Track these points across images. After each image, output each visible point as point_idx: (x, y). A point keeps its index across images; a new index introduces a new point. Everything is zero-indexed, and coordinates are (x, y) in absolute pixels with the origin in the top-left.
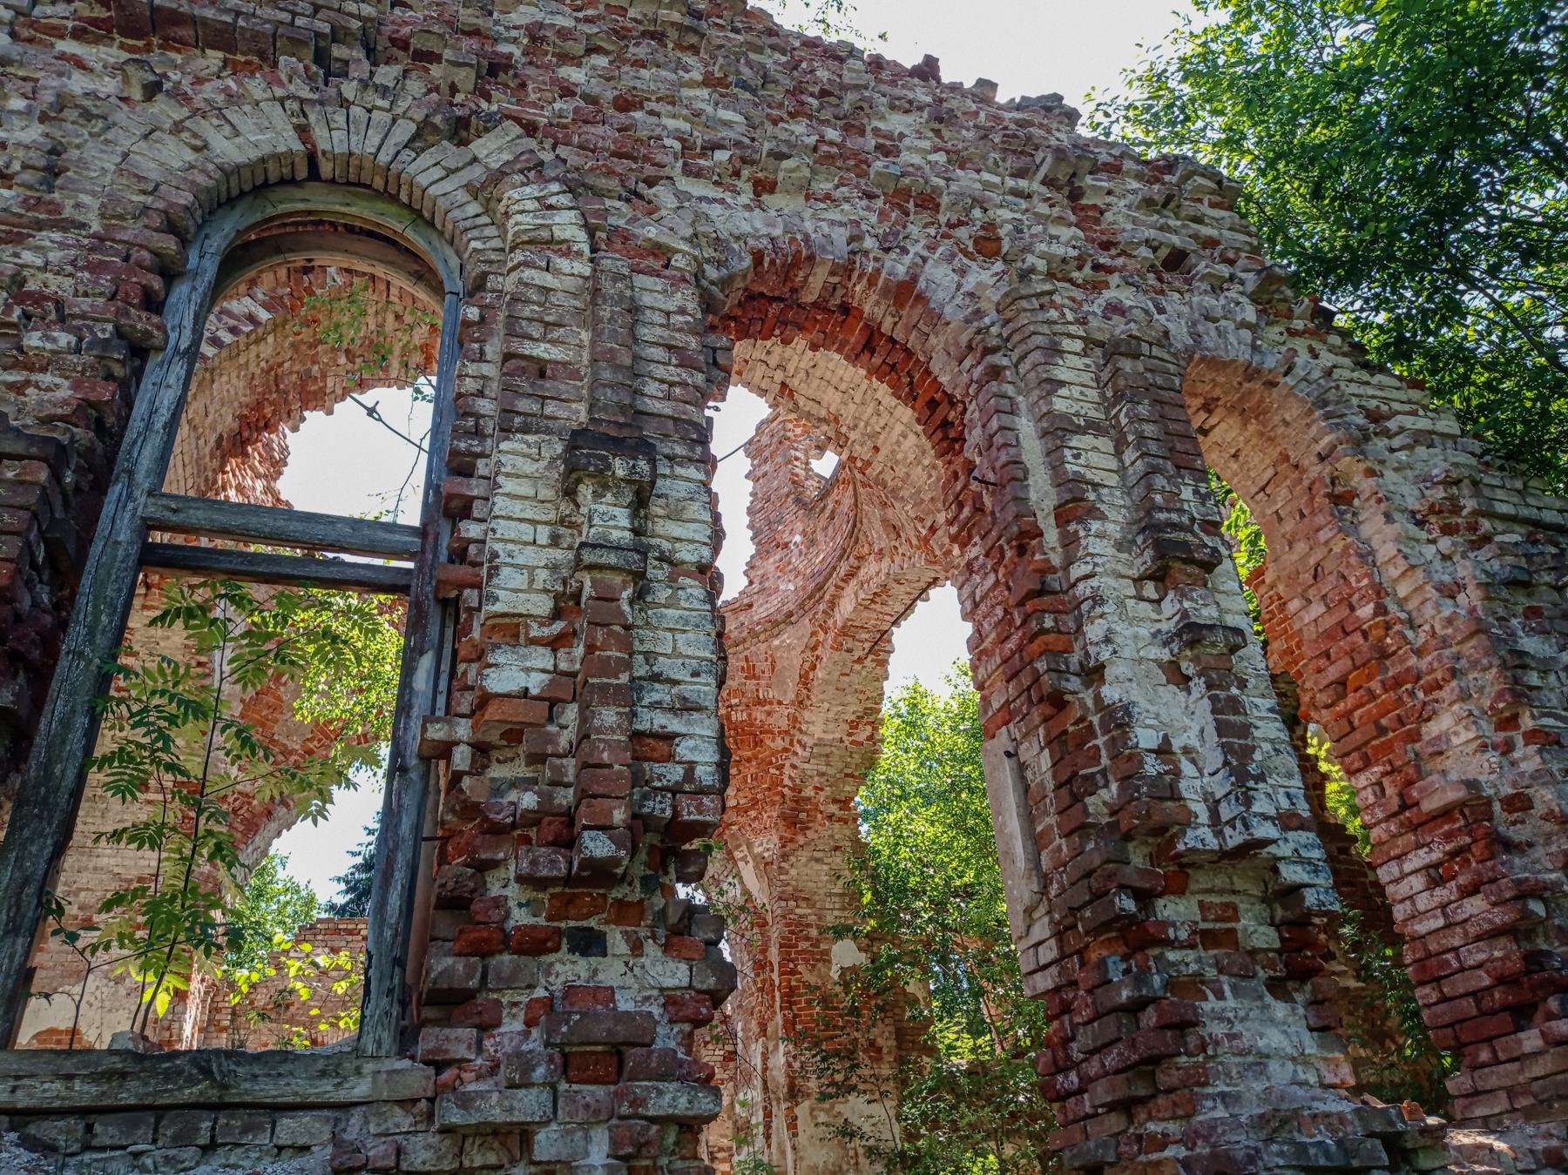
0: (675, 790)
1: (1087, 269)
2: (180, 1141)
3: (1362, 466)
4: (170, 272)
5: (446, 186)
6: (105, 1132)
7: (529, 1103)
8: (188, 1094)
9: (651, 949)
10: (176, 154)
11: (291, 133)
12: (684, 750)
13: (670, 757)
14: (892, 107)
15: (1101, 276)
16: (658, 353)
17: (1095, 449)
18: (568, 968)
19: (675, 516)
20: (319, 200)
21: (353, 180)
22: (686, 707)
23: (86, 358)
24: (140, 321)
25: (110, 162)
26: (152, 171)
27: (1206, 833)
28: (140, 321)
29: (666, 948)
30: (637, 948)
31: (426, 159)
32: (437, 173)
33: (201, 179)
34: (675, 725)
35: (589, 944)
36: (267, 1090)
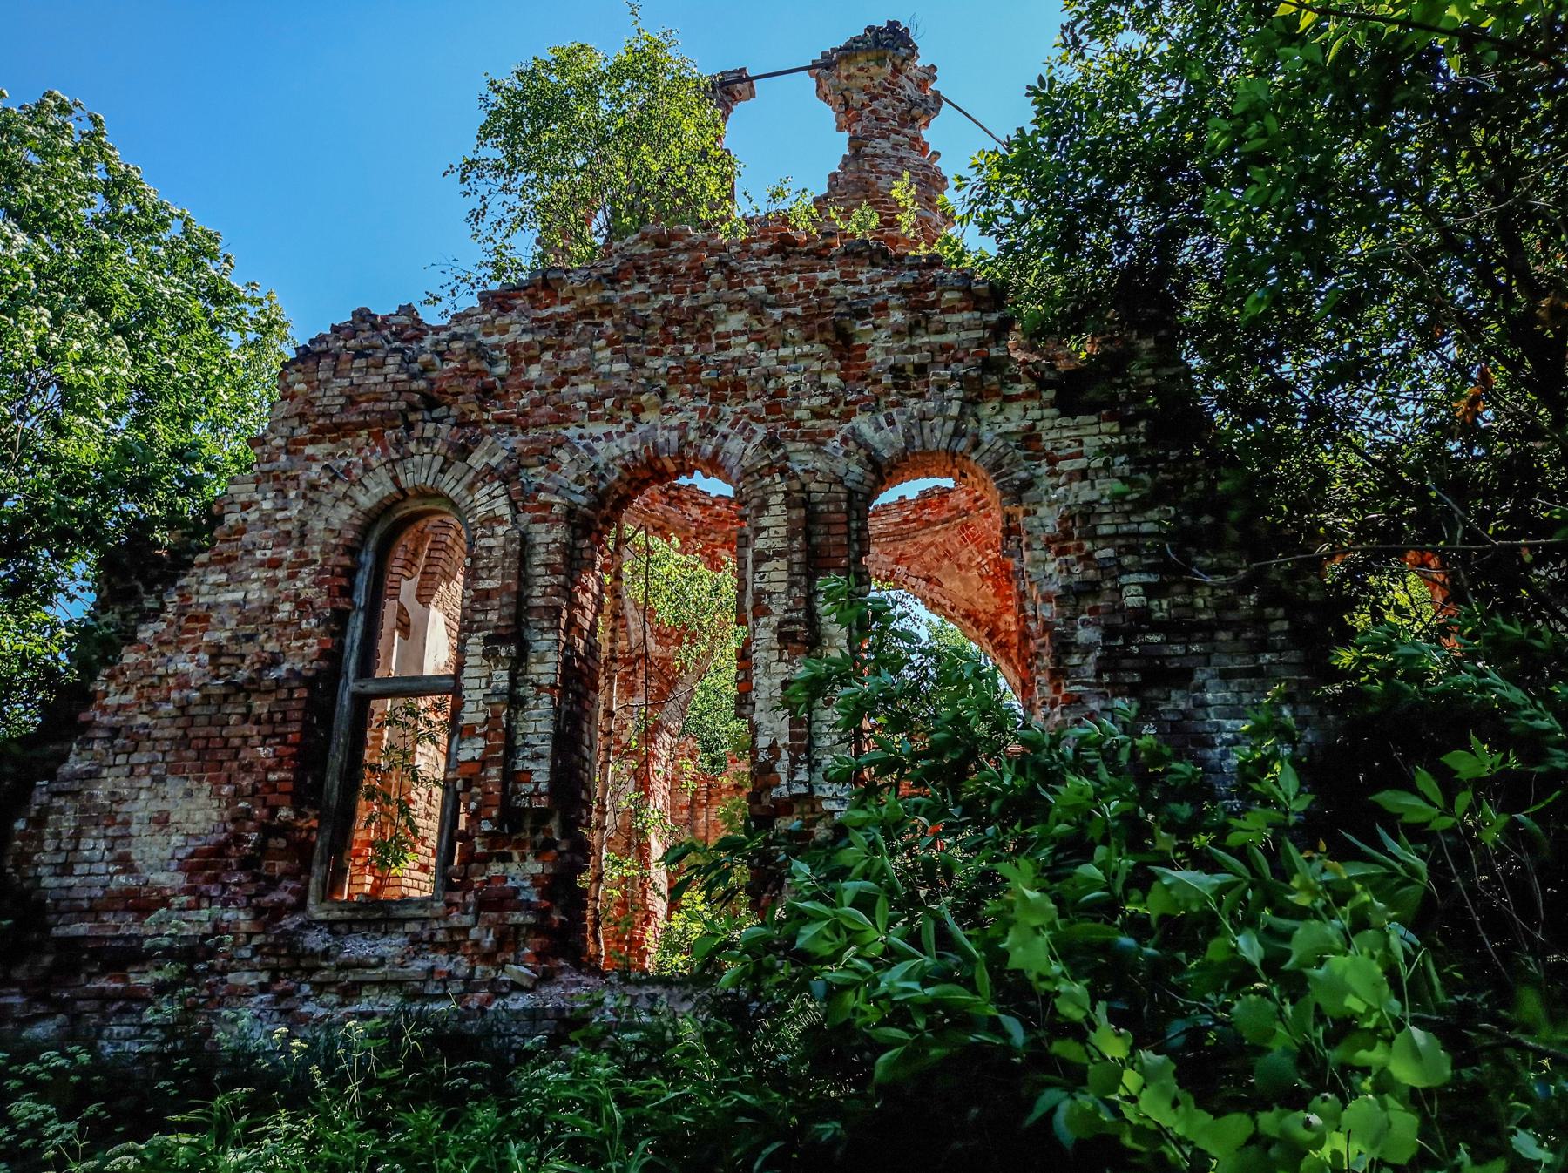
0: (531, 795)
1: (842, 405)
2: (377, 930)
3: (1021, 509)
4: (350, 573)
5: (458, 489)
6: (355, 928)
7: (467, 920)
8: (378, 915)
9: (530, 858)
10: (345, 511)
11: (389, 483)
12: (535, 778)
13: (529, 781)
14: (729, 310)
15: (851, 407)
16: (540, 570)
17: (776, 569)
18: (496, 869)
19: (541, 661)
20: (416, 506)
21: (423, 494)
22: (537, 757)
23: (322, 628)
24: (341, 603)
25: (321, 525)
26: (336, 524)
27: (784, 789)
28: (341, 603)
29: (536, 857)
30: (523, 858)
31: (448, 477)
32: (453, 483)
33: (356, 522)
34: (532, 766)
35: (506, 858)
36: (402, 913)
